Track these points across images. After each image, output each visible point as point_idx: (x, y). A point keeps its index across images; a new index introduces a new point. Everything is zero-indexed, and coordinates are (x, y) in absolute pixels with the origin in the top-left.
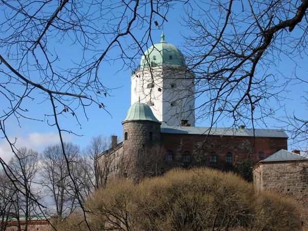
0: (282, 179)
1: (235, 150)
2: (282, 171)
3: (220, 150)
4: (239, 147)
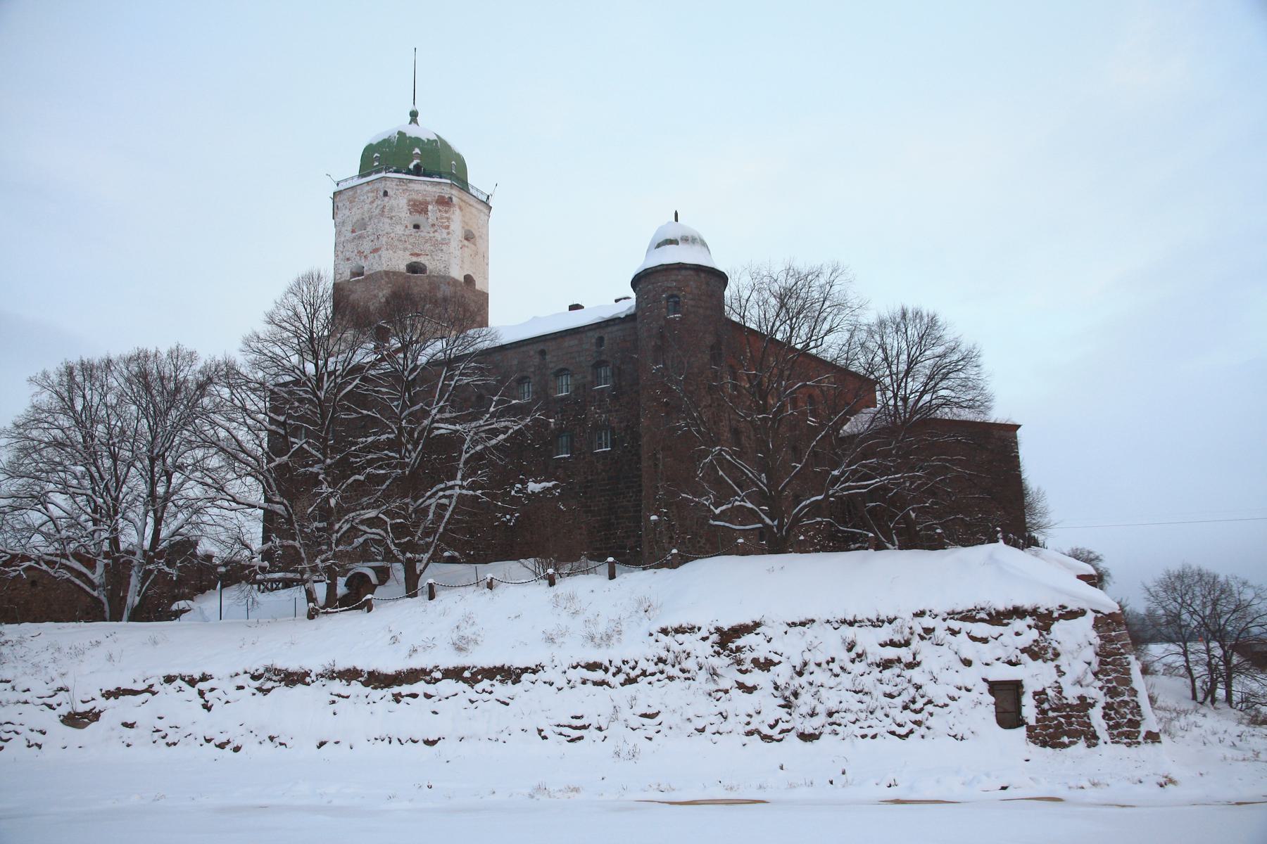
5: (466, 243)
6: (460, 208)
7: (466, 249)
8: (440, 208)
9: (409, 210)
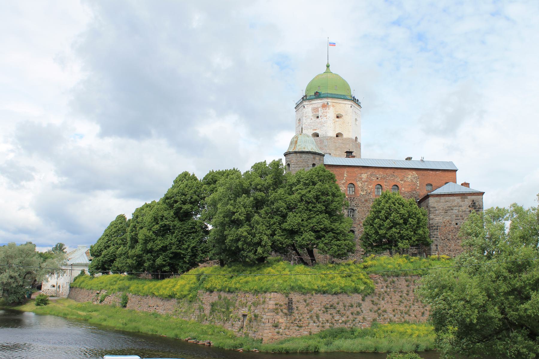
0: (449, 213)
1: (401, 182)
2: (449, 204)
4: (405, 179)
6: (333, 106)
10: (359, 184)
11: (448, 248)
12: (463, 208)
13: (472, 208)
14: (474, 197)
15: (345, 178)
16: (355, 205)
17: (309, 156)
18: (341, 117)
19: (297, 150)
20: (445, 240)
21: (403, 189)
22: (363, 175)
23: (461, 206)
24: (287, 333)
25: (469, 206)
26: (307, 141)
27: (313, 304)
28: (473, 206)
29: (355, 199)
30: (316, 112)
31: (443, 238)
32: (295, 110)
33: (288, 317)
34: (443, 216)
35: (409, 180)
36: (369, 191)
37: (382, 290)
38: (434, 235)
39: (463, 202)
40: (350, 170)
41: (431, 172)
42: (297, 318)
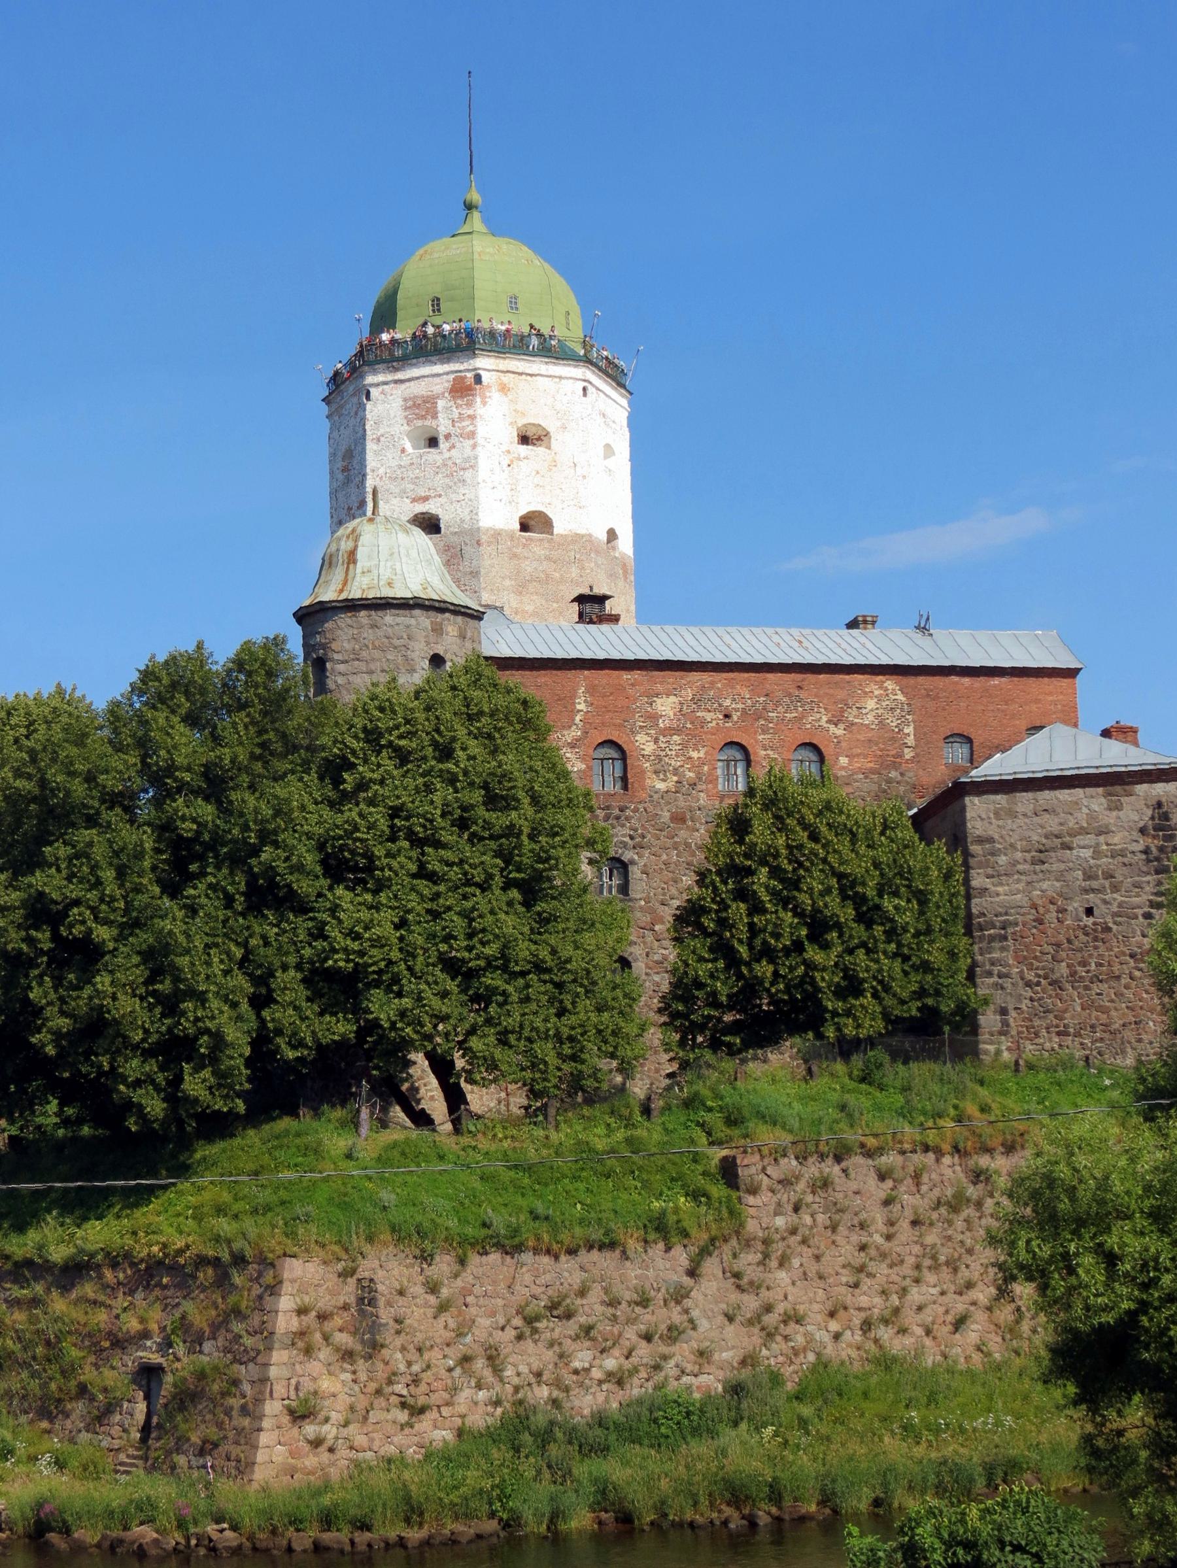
1: (832, 728)
2: (1052, 823)
3: (764, 732)
5: (524, 449)
6: (504, 389)
7: (523, 464)
8: (459, 402)
9: (406, 417)
10: (644, 744)
11: (1055, 1022)
12: (1116, 840)
13: (1154, 837)
14: (1160, 789)
15: (578, 718)
16: (627, 839)
17: (413, 621)
18: (539, 439)
19: (355, 593)
20: (1038, 984)
21: (843, 761)
22: (659, 701)
23: (1103, 831)
24: (360, 1440)
25: (1143, 831)
26: (403, 551)
27: (469, 1299)
28: (1157, 828)
29: (628, 813)
30: (423, 417)
31: (1030, 976)
32: (325, 409)
33: (361, 1365)
34: (1029, 879)
35: (869, 719)
36: (692, 775)
37: (780, 1222)
38: (993, 964)
39: (1115, 813)
40: (603, 677)
41: (966, 681)
42: (402, 1367)
